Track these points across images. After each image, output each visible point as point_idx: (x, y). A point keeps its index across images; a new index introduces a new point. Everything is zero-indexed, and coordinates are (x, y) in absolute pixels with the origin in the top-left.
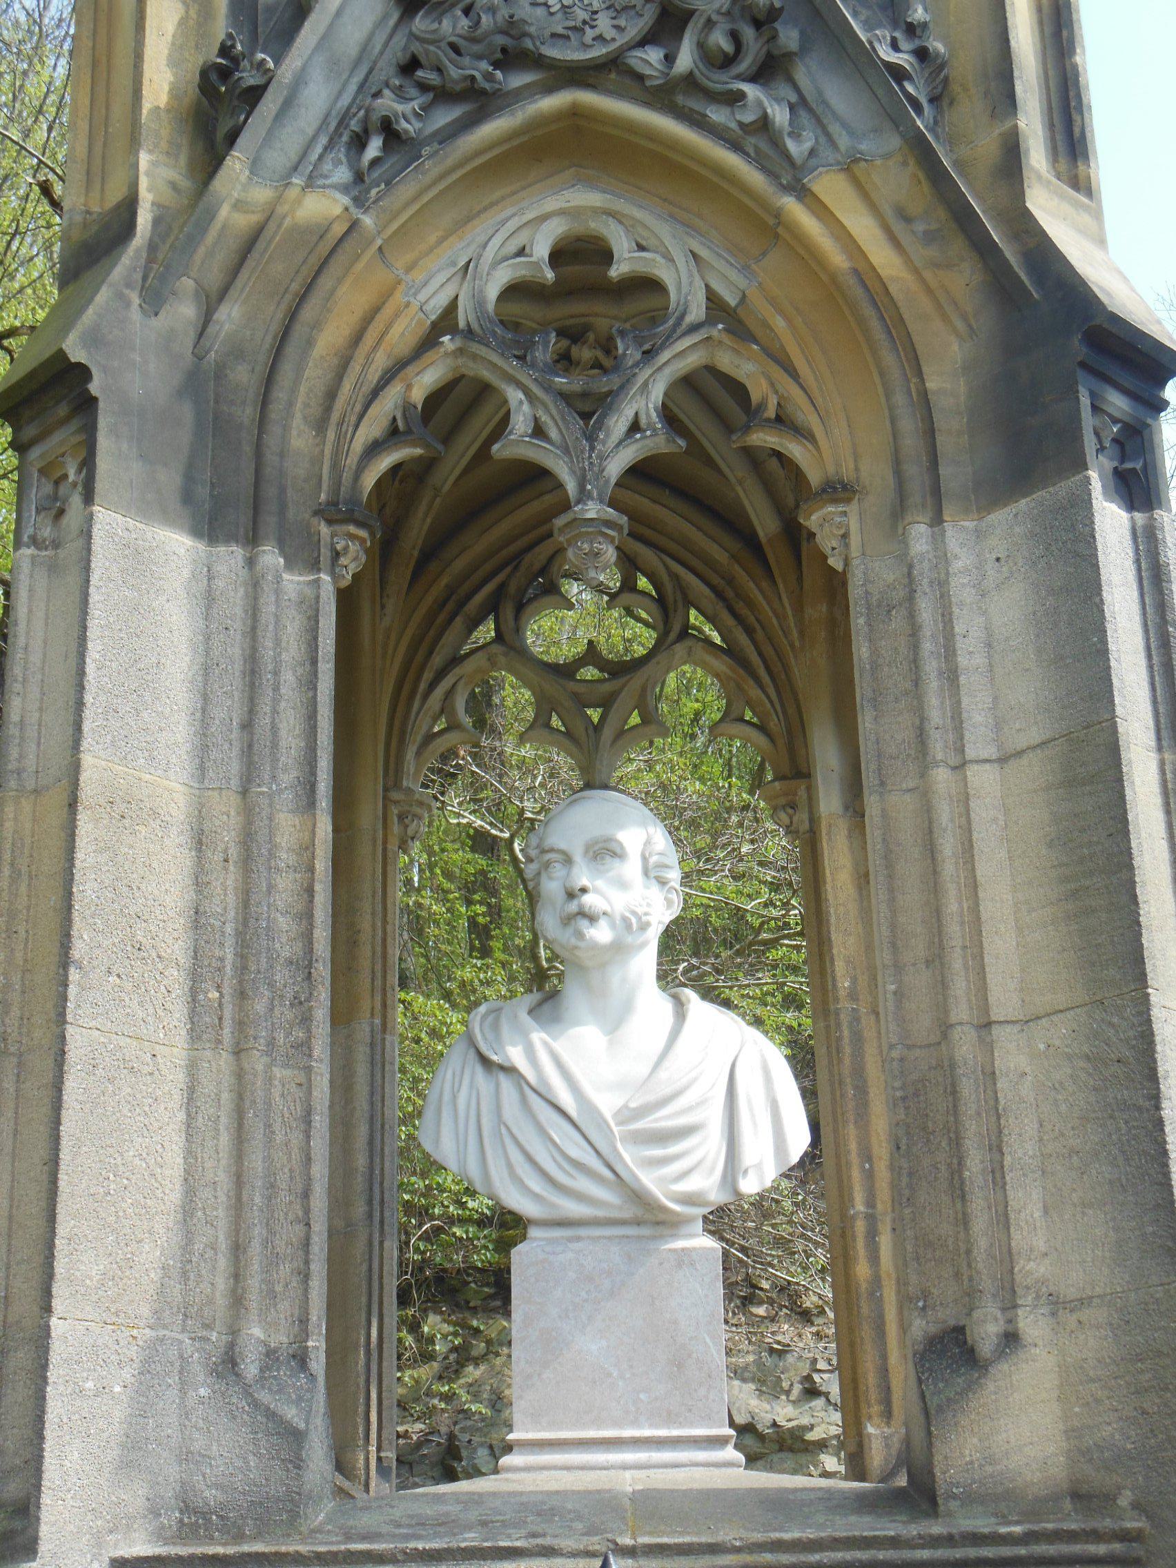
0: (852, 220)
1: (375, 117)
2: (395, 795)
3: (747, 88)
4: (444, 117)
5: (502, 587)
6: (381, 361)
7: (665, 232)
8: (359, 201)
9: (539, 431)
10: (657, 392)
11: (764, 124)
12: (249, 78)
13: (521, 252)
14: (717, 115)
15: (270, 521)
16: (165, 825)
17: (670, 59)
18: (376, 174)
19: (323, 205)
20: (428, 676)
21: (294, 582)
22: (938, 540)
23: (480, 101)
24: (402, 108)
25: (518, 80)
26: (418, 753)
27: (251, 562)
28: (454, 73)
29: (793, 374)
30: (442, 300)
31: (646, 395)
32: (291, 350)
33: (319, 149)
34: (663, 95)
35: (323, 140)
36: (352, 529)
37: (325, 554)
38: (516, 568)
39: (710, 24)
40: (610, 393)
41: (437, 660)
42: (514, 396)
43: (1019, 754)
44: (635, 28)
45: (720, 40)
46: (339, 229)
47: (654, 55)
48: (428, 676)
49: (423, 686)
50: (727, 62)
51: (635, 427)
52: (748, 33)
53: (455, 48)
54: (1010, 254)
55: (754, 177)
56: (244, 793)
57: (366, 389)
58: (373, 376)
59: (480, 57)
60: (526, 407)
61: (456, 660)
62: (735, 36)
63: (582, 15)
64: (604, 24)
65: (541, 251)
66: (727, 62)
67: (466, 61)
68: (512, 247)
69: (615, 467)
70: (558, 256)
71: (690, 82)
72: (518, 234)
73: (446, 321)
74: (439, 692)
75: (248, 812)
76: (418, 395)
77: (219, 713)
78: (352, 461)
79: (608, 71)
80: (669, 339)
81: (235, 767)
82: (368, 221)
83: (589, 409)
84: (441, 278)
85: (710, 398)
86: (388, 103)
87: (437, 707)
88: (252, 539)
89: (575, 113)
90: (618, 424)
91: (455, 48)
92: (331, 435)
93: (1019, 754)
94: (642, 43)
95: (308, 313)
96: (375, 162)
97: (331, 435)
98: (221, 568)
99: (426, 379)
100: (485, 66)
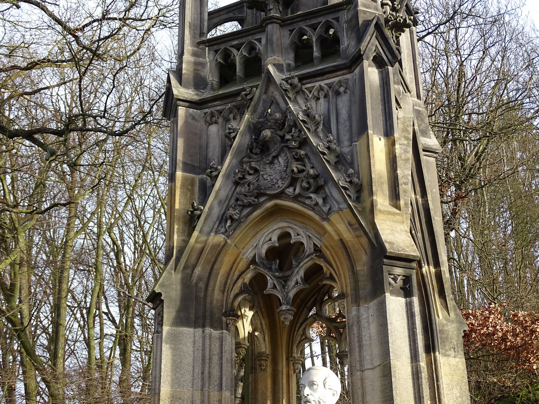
0: (339, 226)
1: (228, 216)
2: (291, 359)
3: (312, 195)
4: (245, 212)
5: (316, 298)
6: (237, 273)
7: (301, 231)
8: (228, 237)
9: (275, 287)
10: (302, 273)
11: (317, 204)
12: (198, 212)
13: (270, 240)
14: (308, 202)
15: (208, 321)
16: (183, 401)
17: (295, 190)
18: (231, 229)
19: (220, 238)
20: (298, 325)
21: (216, 333)
22: (358, 311)
23: (255, 207)
24: (234, 213)
25: (262, 199)
26: (297, 346)
27: (203, 332)
28: (245, 201)
29: (331, 266)
30: (252, 255)
31: (299, 275)
32: (212, 278)
33: (217, 225)
34: (296, 198)
35: (218, 222)
36: (231, 318)
37: (224, 325)
38: (319, 293)
39: (303, 181)
40: (289, 275)
41: (301, 320)
42: (269, 278)
43: (376, 367)
44: (287, 182)
45: (305, 184)
46: (222, 243)
47: (291, 190)
48: (298, 325)
49: (297, 328)
50: (308, 189)
51: (297, 283)
52: (312, 181)
53: (246, 196)
54: (371, 236)
55: (317, 218)
56: (202, 390)
57: (233, 281)
58: (235, 278)
59: (251, 196)
60: (271, 281)
61: (306, 319)
62: (308, 183)
63: (275, 181)
64: (280, 182)
65: (275, 238)
66: (308, 189)
67: (248, 198)
68: (268, 239)
69: (291, 294)
70: (280, 238)
71: (300, 195)
72: (268, 236)
73: (253, 261)
74: (301, 329)
75: (203, 395)
76: (247, 281)
77: (196, 371)
78: (230, 300)
79: (281, 195)
80: (302, 260)
81: (200, 384)
82: (229, 241)
83: (285, 280)
84: (250, 250)
85: (314, 272)
86: (231, 212)
87: (302, 333)
88: (204, 326)
89: (276, 205)
90: (292, 283)
91: (246, 196)
92: (226, 294)
93: (376, 367)
94: (288, 187)
95: (216, 267)
96: (229, 226)
97: (226, 294)
98: (197, 334)
99: (248, 276)
100: (253, 198)
